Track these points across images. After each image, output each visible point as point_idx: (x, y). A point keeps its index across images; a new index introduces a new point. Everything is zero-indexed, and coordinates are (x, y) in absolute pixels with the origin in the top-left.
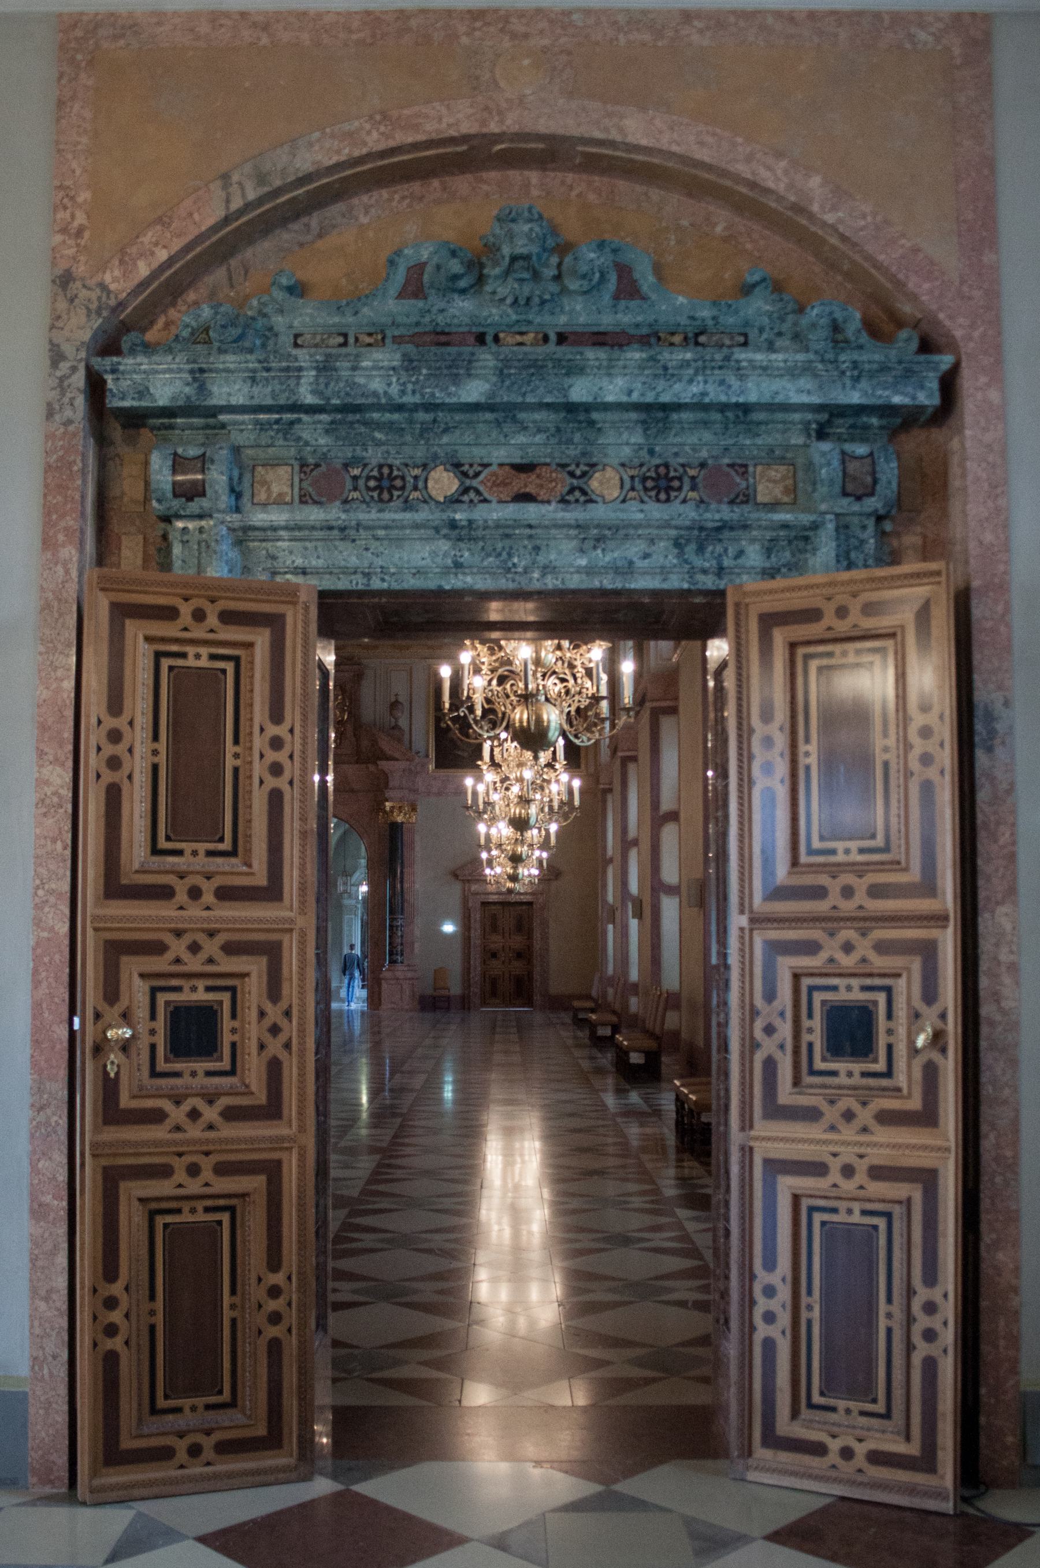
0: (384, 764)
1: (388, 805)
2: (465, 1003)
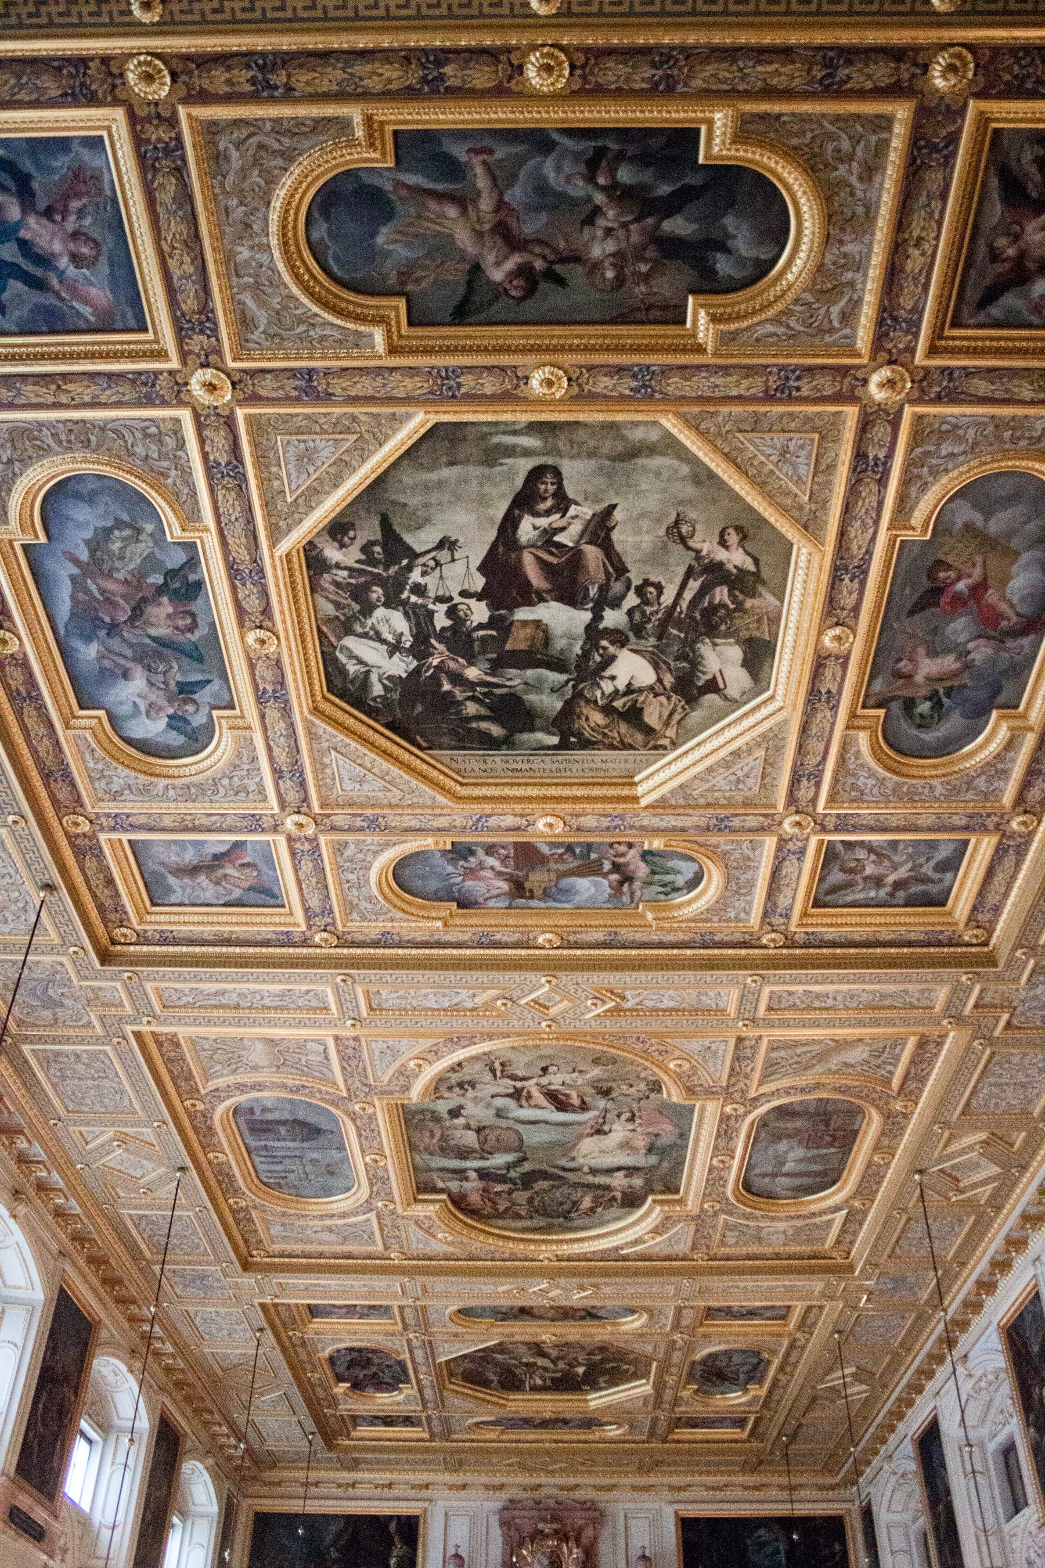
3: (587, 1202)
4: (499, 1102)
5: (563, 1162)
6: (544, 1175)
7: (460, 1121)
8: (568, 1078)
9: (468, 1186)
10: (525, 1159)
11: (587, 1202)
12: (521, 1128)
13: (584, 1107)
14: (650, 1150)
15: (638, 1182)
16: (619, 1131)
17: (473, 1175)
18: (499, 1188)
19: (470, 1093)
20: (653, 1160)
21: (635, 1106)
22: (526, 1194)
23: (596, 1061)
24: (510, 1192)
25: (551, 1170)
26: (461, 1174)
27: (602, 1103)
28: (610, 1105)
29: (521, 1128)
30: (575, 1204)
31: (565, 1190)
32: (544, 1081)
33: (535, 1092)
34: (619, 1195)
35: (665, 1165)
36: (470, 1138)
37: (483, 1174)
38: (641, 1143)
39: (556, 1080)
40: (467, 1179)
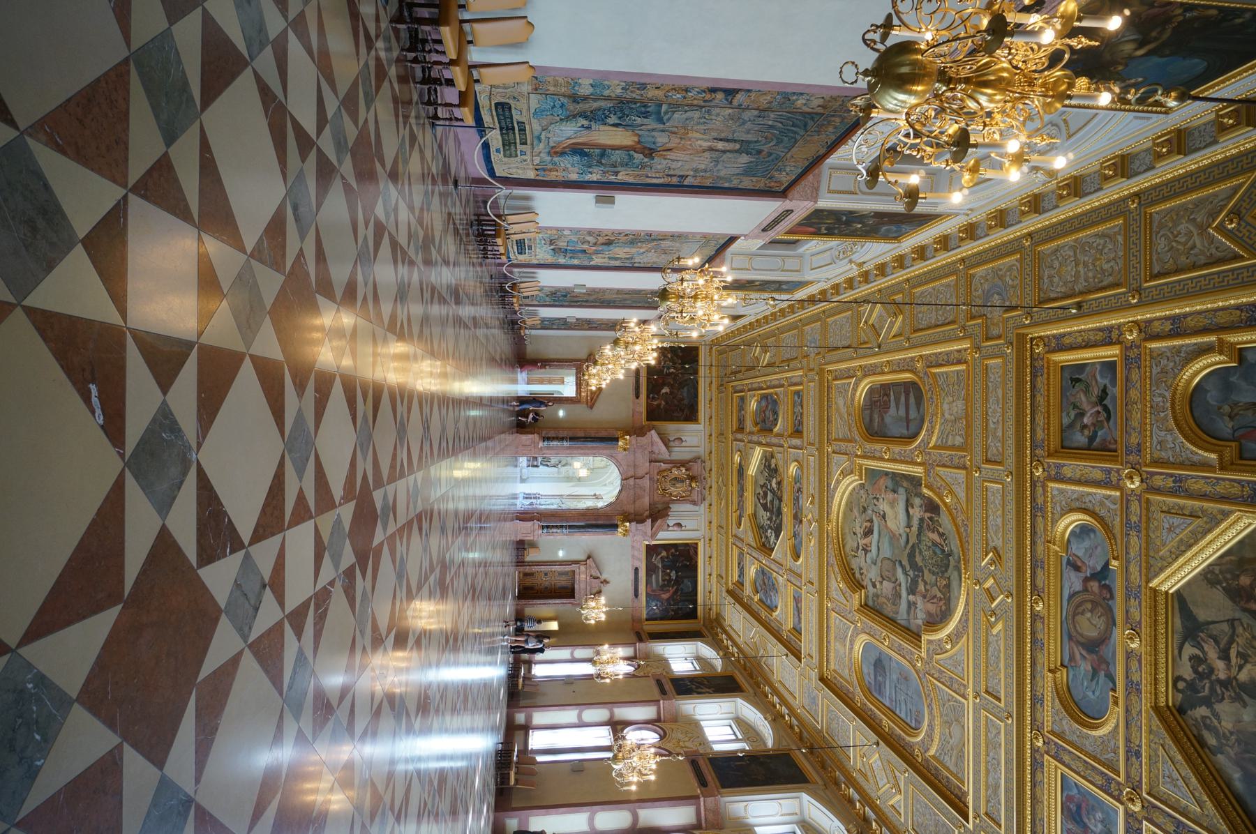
0: (649, 521)
2: (520, 562)
3: (935, 537)
4: (869, 561)
5: (903, 541)
6: (911, 556)
8: (858, 525)
9: (920, 604)
11: (935, 537)
12: (881, 556)
13: (871, 521)
14: (895, 491)
16: (884, 506)
17: (911, 597)
18: (921, 587)
20: (901, 490)
22: (926, 572)
24: (926, 583)
25: (907, 550)
26: (911, 605)
27: (869, 512)
29: (881, 556)
30: (935, 544)
31: (923, 547)
33: (865, 541)
34: (927, 515)
35: (905, 484)
36: (887, 586)
37: (912, 590)
38: (891, 496)
39: (860, 531)
40: (915, 604)
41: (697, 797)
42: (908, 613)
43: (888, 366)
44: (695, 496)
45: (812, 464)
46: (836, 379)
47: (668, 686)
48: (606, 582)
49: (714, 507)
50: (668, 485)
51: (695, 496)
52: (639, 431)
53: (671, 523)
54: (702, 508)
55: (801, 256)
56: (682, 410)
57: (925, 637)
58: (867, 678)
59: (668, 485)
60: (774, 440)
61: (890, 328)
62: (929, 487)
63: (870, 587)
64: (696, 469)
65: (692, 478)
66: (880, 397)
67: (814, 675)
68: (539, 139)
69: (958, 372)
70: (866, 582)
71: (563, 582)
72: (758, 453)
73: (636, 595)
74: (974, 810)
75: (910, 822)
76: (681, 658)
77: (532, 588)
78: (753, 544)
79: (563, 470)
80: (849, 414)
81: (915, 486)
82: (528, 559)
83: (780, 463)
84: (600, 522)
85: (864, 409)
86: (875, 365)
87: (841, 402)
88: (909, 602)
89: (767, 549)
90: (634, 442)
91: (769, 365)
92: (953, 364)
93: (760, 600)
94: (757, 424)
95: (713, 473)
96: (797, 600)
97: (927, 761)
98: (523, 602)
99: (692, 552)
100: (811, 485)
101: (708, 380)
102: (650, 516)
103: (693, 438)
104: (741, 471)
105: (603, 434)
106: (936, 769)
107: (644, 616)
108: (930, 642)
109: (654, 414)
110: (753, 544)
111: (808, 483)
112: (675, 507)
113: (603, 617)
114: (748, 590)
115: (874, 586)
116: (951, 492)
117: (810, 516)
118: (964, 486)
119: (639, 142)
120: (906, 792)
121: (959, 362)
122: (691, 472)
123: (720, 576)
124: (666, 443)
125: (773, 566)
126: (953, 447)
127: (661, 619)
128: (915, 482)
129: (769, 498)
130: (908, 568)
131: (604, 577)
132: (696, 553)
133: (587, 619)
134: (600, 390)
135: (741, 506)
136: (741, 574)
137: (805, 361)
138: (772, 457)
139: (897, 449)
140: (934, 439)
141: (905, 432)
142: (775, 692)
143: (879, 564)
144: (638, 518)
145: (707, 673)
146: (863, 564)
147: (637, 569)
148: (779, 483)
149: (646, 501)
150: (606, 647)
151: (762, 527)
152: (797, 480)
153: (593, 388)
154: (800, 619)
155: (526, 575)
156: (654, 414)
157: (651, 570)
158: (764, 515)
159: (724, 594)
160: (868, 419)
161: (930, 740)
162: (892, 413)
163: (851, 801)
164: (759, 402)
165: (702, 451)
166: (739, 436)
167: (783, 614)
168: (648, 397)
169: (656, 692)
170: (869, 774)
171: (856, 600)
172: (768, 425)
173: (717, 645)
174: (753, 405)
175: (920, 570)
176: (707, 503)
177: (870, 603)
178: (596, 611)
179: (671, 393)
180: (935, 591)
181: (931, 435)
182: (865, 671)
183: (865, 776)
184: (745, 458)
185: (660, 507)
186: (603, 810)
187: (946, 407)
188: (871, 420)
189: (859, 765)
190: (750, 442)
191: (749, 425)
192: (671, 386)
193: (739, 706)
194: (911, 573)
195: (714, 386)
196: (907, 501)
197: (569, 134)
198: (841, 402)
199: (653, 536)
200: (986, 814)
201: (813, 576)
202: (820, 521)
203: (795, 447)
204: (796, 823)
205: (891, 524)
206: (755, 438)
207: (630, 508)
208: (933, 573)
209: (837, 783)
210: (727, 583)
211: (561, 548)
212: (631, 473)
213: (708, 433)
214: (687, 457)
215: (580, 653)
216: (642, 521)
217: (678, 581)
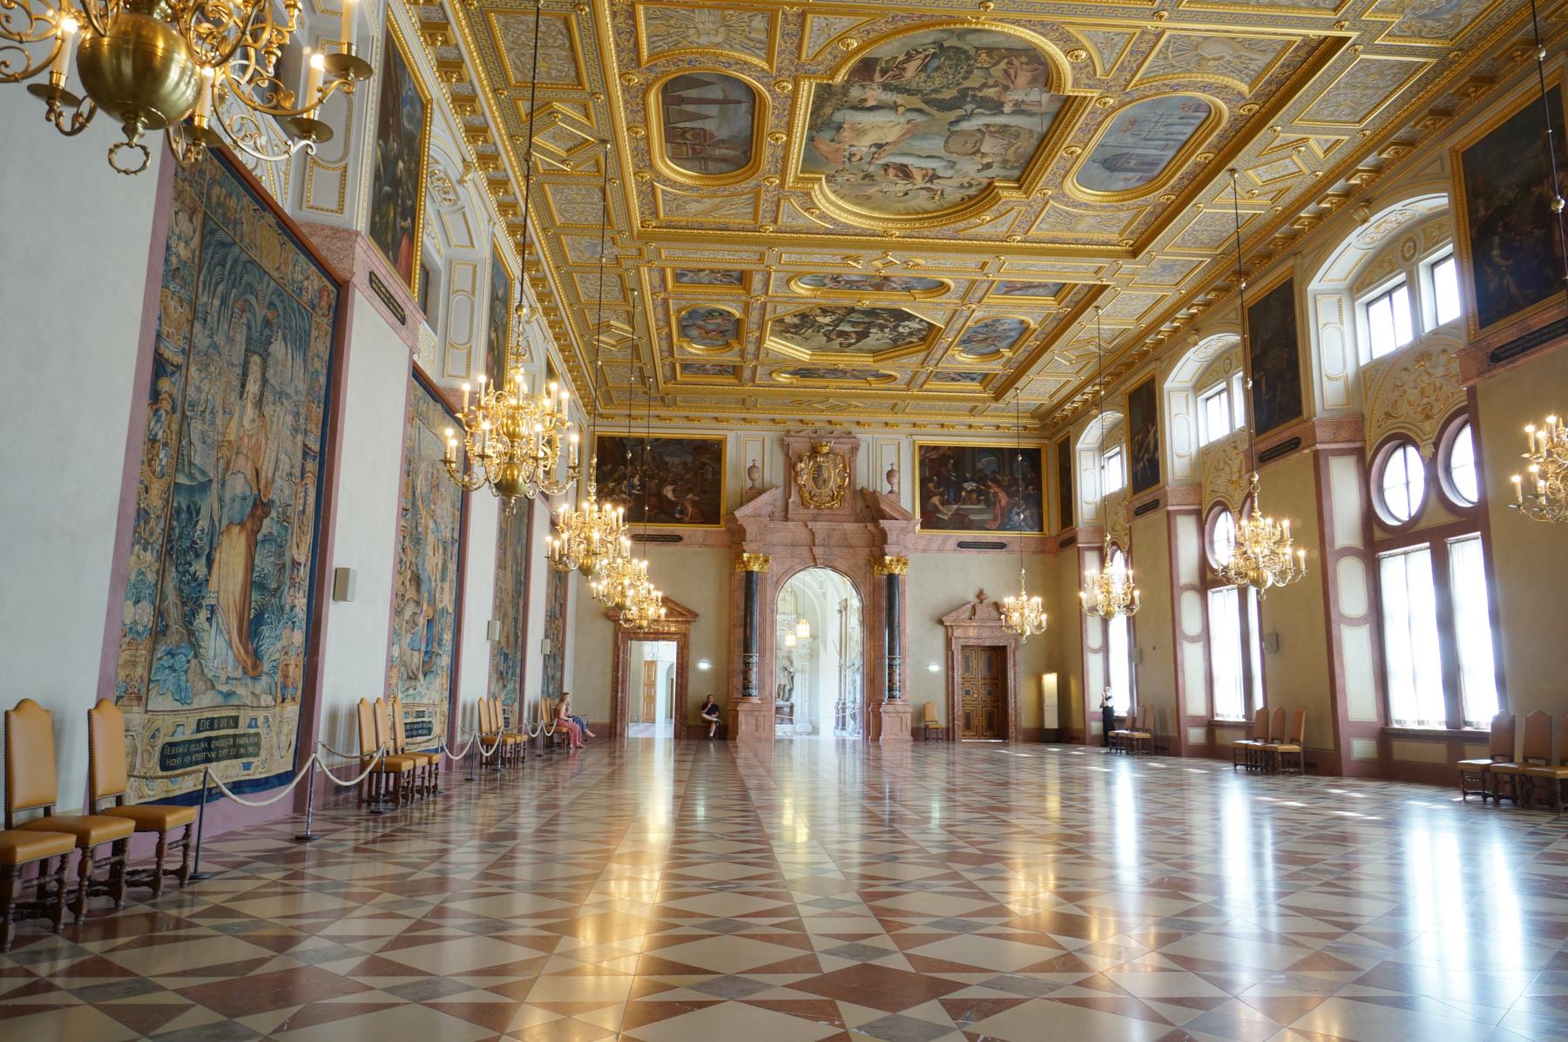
0: (884, 523)
1: (888, 558)
2: (948, 736)
3: (912, 67)
5: (919, 118)
7: (985, 161)
8: (893, 188)
9: (1020, 96)
10: (951, 123)
12: (943, 153)
13: (886, 167)
14: (839, 128)
15: (855, 93)
16: (863, 145)
17: (1007, 109)
18: (991, 92)
19: (965, 181)
20: (838, 117)
21: (847, 165)
22: (967, 84)
23: (869, 197)
24: (985, 85)
25: (933, 111)
26: (1019, 110)
27: (872, 169)
28: (866, 167)
29: (943, 153)
30: (923, 68)
31: (928, 87)
32: (909, 187)
34: (877, 77)
35: (828, 110)
37: (996, 107)
38: (846, 134)
39: (902, 186)
40: (1017, 103)
41: (1316, 454)
42: (1031, 114)
43: (637, 131)
44: (844, 448)
45: (794, 258)
46: (655, 213)
47: (1146, 497)
48: (980, 595)
49: (862, 418)
50: (826, 491)
51: (844, 448)
52: (737, 537)
53: (887, 488)
54: (864, 436)
55: (450, 263)
56: (703, 465)
57: (1069, 91)
58: (1133, 183)
59: (826, 491)
60: (755, 316)
61: (573, 122)
62: (833, 72)
63: (991, 173)
64: (799, 445)
65: (815, 452)
66: (688, 144)
67: (1127, 266)
68: (229, 695)
69: (648, 18)
70: (983, 178)
71: (979, 665)
72: (776, 345)
73: (1001, 546)
74: (1330, 28)
75: (1350, 126)
76: (1101, 476)
77: (990, 717)
78: (923, 355)
79: (798, 664)
80: (714, 195)
81: (832, 94)
82: (942, 723)
83: (792, 308)
84: (884, 603)
85: (705, 171)
86: (635, 149)
87: (694, 207)
88: (1014, 113)
89: (929, 335)
90: (753, 546)
91: (631, 323)
92: (635, 26)
93: (1010, 347)
94: (727, 344)
95: (806, 417)
96: (1011, 289)
97: (1257, 97)
98: (1012, 730)
99: (934, 455)
100: (827, 260)
101: (654, 422)
102: (875, 520)
103: (748, 449)
104: (804, 372)
105: (740, 597)
106: (1269, 83)
107: (1035, 534)
108: (1076, 83)
109: (709, 512)
110: (923, 355)
111: (824, 264)
112: (862, 481)
113: (1037, 600)
114: (995, 367)
115: (988, 166)
116: (841, 38)
117: (878, 264)
118: (832, 18)
119: (242, 524)
120: (1304, 130)
121: (632, 15)
122: (804, 453)
123: (972, 411)
124: (756, 493)
125: (958, 325)
126: (770, 32)
127: (1040, 506)
128: (824, 95)
129: (847, 328)
130: (960, 112)
131: (972, 599)
132: (935, 448)
133: (1039, 626)
134: (665, 601)
135: (860, 374)
136: (969, 376)
137: (625, 264)
138: (781, 321)
139: (770, 121)
140: (756, 61)
141: (744, 107)
142: (1153, 327)
143: (954, 157)
144: (878, 542)
145: (1124, 435)
146: (955, 182)
147: (962, 545)
148: (825, 312)
149: (850, 527)
150: (1083, 595)
151: (895, 341)
152: (819, 282)
153: (663, 611)
154: (1040, 285)
155: (968, 726)
156: (709, 512)
157: (961, 522)
158: (876, 338)
159: (1001, 404)
160: (723, 166)
161: (1227, 90)
162: (713, 127)
163: (1320, 216)
164: (692, 340)
165: (770, 435)
166: (747, 374)
167: (1033, 312)
168: (679, 521)
169: (1156, 517)
170: (1278, 186)
171: (1010, 196)
172: (730, 326)
173: (1080, 419)
174: (696, 349)
175: (963, 94)
176: (854, 429)
177: (1016, 173)
178: (1027, 612)
179: (674, 483)
180: (997, 72)
181: (751, 67)
182: (1121, 185)
183: (1281, 192)
184: (781, 364)
185: (860, 505)
186: (1337, 602)
187: (704, 40)
188: (724, 160)
189: (1265, 201)
190: (757, 357)
191: (730, 357)
192: (663, 482)
193: (1174, 385)
194: (969, 107)
195: (663, 412)
196: (854, 108)
197: (221, 644)
198: (694, 207)
199: (907, 517)
200: (1335, 10)
201: (972, 261)
202: (886, 248)
203: (767, 284)
204: (1353, 300)
205: (892, 135)
206: (751, 348)
207: (863, 553)
208: (969, 72)
209: (1293, 236)
210: (984, 400)
211: (925, 669)
212: (804, 551)
213: (743, 425)
214: (779, 459)
215: (1093, 638)
216: (883, 536)
217: (980, 479)
